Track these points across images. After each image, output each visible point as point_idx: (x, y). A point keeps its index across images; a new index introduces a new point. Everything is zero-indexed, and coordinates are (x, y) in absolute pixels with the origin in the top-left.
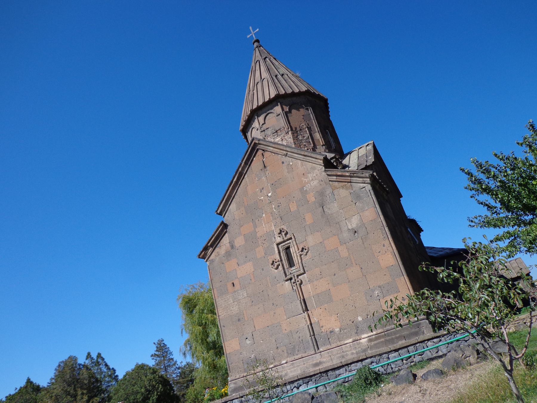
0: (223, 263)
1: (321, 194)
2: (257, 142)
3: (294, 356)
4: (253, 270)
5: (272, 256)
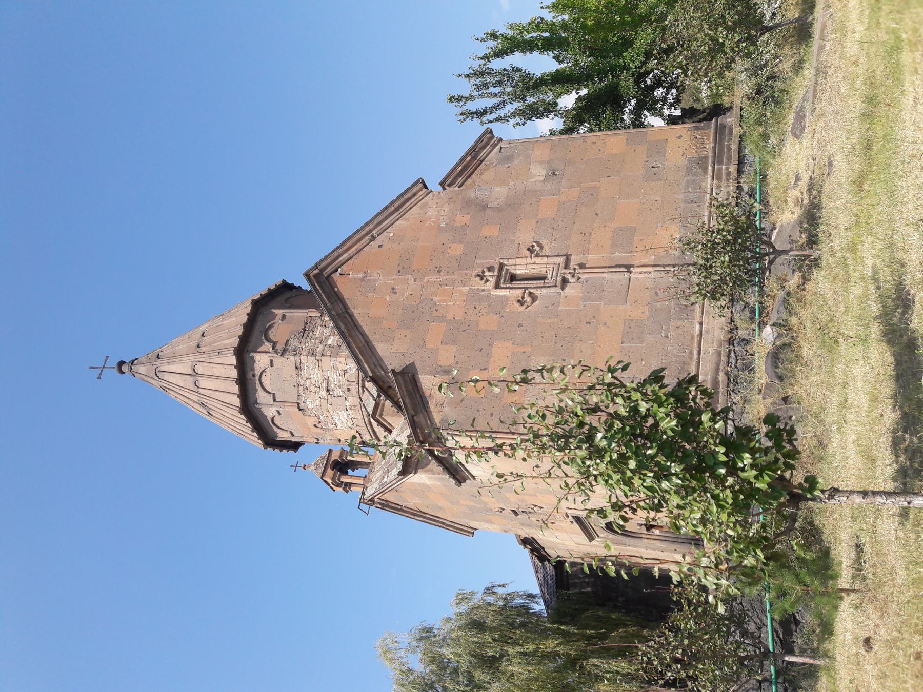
0: (462, 401)
1: (468, 204)
2: (317, 271)
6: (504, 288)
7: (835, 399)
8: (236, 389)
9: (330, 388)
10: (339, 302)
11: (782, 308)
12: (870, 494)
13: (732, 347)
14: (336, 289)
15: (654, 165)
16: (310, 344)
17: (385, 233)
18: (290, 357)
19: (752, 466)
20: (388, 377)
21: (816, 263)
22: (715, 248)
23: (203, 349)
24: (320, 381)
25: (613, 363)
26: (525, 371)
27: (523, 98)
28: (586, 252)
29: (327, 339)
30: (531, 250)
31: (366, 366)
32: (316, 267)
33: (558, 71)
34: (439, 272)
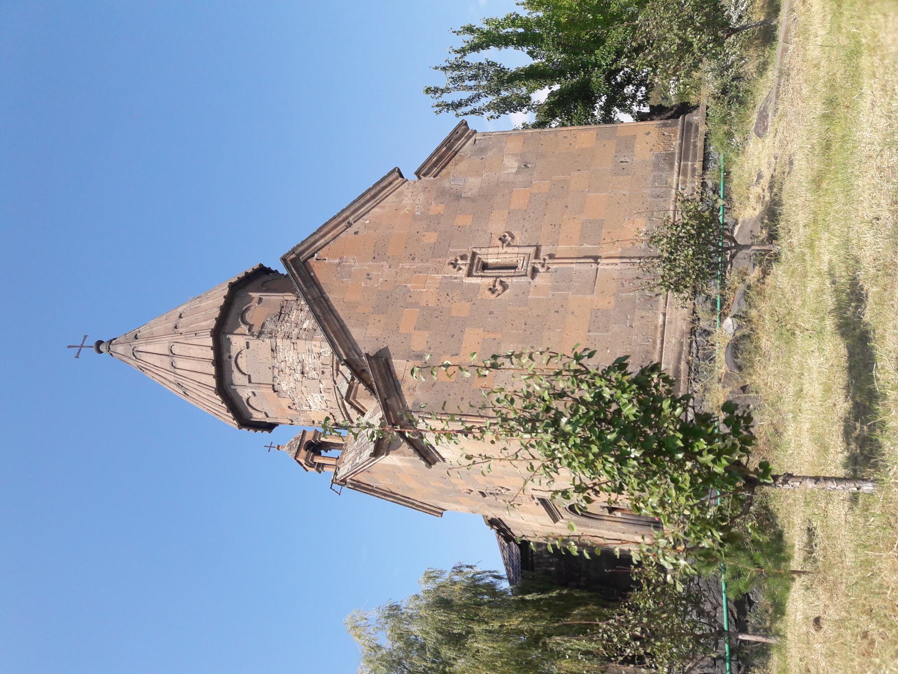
0: (433, 385)
1: (442, 193)
2: (293, 256)
3: (658, 301)
4: (482, 329)
5: (481, 290)
6: (476, 276)
7: (791, 389)
8: (212, 370)
9: (304, 370)
10: (315, 286)
11: (742, 301)
12: (822, 480)
13: (693, 337)
14: (312, 274)
15: (623, 159)
16: (286, 327)
17: (361, 220)
18: (265, 339)
19: (710, 452)
20: (362, 360)
21: (776, 257)
22: (679, 242)
23: (180, 330)
24: (296, 364)
25: (579, 350)
26: (495, 357)
27: (498, 92)
28: (555, 243)
29: (303, 322)
30: (502, 240)
31: (341, 350)
32: (293, 251)
33: (531, 66)
34: (413, 259)
